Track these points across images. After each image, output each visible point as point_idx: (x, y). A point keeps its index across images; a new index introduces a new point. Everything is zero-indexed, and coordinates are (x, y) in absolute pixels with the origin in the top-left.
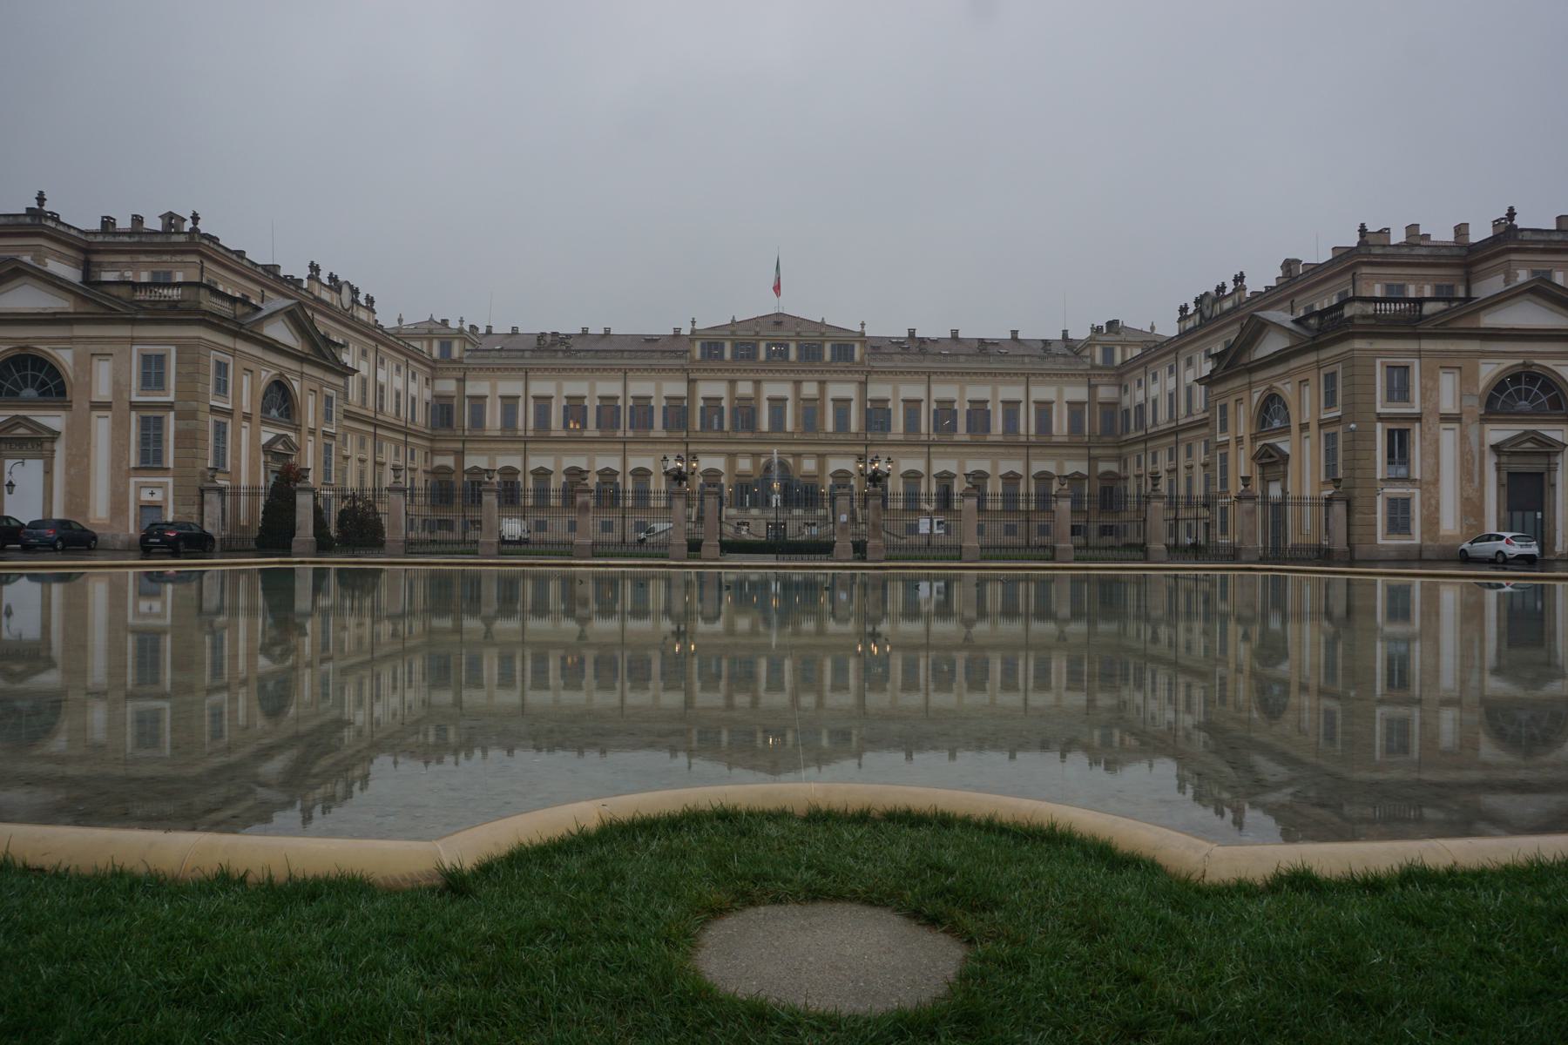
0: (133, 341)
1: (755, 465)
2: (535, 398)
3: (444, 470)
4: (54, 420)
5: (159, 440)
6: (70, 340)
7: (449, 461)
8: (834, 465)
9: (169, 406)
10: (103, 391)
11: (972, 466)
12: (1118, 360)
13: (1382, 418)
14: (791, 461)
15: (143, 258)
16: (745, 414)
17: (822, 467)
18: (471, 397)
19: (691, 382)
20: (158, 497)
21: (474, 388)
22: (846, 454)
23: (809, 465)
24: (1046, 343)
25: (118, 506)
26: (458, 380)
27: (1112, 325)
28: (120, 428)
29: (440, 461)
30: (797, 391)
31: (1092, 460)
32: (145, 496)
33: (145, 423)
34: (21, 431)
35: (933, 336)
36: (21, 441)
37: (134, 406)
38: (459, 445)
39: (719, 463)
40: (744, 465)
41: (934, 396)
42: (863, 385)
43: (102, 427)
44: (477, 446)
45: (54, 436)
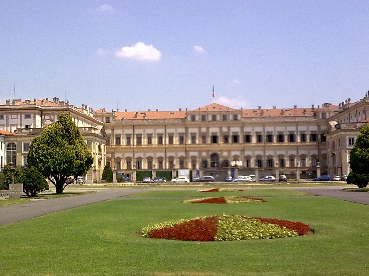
1: (208, 154)
11: (279, 153)
12: (328, 117)
13: (348, 149)
14: (219, 153)
15: (55, 112)
18: (116, 135)
19: (187, 128)
22: (237, 150)
23: (225, 154)
24: (305, 110)
26: (112, 129)
30: (221, 130)
31: (319, 150)
35: (267, 108)
40: (204, 154)
42: (242, 128)
44: (118, 150)
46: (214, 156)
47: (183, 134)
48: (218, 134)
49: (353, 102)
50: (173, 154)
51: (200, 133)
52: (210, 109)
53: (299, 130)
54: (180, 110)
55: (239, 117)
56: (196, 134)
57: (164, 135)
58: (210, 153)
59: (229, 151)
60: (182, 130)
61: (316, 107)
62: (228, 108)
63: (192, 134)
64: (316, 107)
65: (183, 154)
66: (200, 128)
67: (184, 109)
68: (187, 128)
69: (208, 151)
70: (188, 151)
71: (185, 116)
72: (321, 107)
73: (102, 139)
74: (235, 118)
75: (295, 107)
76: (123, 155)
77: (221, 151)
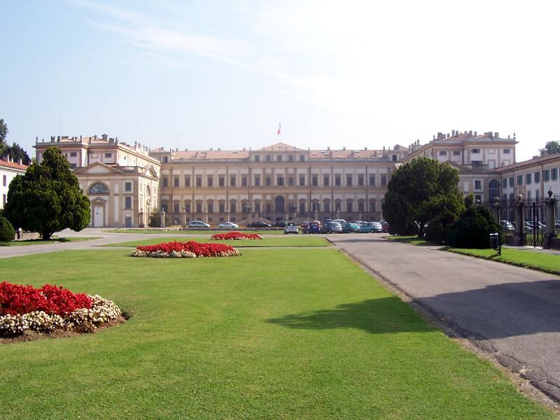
0: (124, 179)
1: (272, 197)
2: (197, 176)
3: (165, 200)
4: (105, 198)
5: (130, 202)
6: (108, 180)
7: (167, 198)
8: (300, 197)
9: (132, 194)
10: (117, 191)
11: (348, 196)
14: (284, 196)
16: (268, 181)
17: (295, 197)
19: (250, 169)
20: (130, 215)
21: (176, 172)
22: (304, 193)
23: (291, 197)
25: (121, 217)
27: (397, 147)
28: (121, 200)
29: (164, 198)
32: (127, 215)
33: (127, 198)
34: (98, 201)
35: (336, 149)
36: (98, 204)
37: (124, 195)
38: (170, 192)
39: (259, 197)
40: (269, 197)
41: (334, 173)
43: (116, 199)
45: (106, 201)
46: (280, 200)
47: (246, 175)
48: (284, 176)
49: (422, 143)
50: (235, 197)
51: (264, 174)
52: (276, 149)
53: (368, 173)
54: (244, 150)
55: (306, 159)
56: (260, 175)
57: (226, 177)
58: (275, 196)
59: (295, 195)
60: (245, 171)
61: (387, 149)
62: (295, 148)
63: (255, 175)
64: (387, 149)
65: (246, 197)
66: (264, 169)
67: (248, 149)
68: (250, 169)
69: (273, 194)
70: (252, 194)
71: (248, 156)
72: (392, 149)
73: (151, 179)
74: (302, 158)
75: (366, 149)
76: (182, 198)
77: (287, 194)
